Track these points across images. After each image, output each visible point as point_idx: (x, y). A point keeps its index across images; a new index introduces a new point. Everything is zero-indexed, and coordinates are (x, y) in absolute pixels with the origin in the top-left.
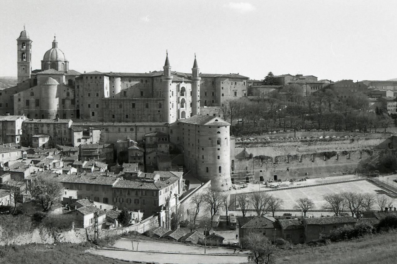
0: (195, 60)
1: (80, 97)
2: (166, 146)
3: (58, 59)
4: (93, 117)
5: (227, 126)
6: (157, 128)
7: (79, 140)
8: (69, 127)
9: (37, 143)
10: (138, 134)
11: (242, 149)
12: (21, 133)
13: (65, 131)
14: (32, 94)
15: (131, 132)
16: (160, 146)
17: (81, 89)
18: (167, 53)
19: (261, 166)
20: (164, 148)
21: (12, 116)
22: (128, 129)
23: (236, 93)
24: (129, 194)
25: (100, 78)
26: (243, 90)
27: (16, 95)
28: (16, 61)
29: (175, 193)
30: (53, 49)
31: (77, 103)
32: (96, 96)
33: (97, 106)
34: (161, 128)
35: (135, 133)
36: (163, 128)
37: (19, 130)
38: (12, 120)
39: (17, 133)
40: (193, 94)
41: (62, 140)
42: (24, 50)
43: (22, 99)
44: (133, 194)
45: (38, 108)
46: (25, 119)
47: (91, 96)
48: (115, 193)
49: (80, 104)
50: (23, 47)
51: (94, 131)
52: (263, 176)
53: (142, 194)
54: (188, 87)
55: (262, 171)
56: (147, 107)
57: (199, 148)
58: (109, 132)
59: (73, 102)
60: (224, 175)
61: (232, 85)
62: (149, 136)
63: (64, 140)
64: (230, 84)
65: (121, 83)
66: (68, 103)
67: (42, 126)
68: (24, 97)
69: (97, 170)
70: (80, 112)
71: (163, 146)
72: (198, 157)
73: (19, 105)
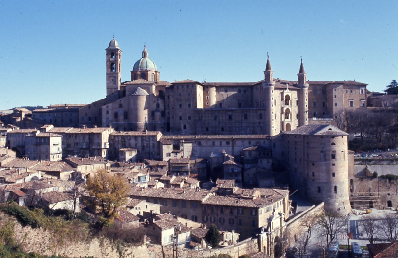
0: (301, 64)
2: (268, 162)
3: (148, 69)
5: (344, 137)
6: (257, 141)
7: (169, 155)
8: (158, 140)
9: (124, 157)
10: (235, 148)
11: (363, 167)
12: (108, 147)
13: (153, 144)
14: (121, 106)
15: (227, 145)
16: (261, 162)
17: (171, 99)
18: (268, 56)
19: (389, 188)
20: (266, 163)
21: (99, 129)
22: (224, 143)
23: (352, 103)
24: (222, 212)
26: (360, 99)
27: (104, 107)
29: (279, 212)
30: (143, 59)
31: (167, 115)
32: (187, 106)
33: (189, 118)
34: (262, 141)
35: (231, 147)
36: (264, 142)
37: (105, 143)
38: (98, 132)
39: (103, 146)
40: (300, 103)
41: (150, 154)
42: (113, 60)
43: (110, 112)
44: (227, 212)
46: (112, 131)
47: (182, 107)
48: (205, 210)
49: (171, 116)
51: (185, 145)
52: (392, 201)
53: (238, 212)
54: (293, 95)
55: (390, 194)
56: (246, 118)
57: (308, 164)
58: (201, 146)
59: (163, 114)
60: (341, 196)
61: (346, 94)
62: (247, 150)
63: (152, 154)
64: (345, 92)
65: (217, 94)
66: (158, 115)
67: (130, 139)
68: (112, 110)
69: (186, 186)
70: (171, 124)
71: (265, 161)
72: (308, 174)
73: (107, 119)
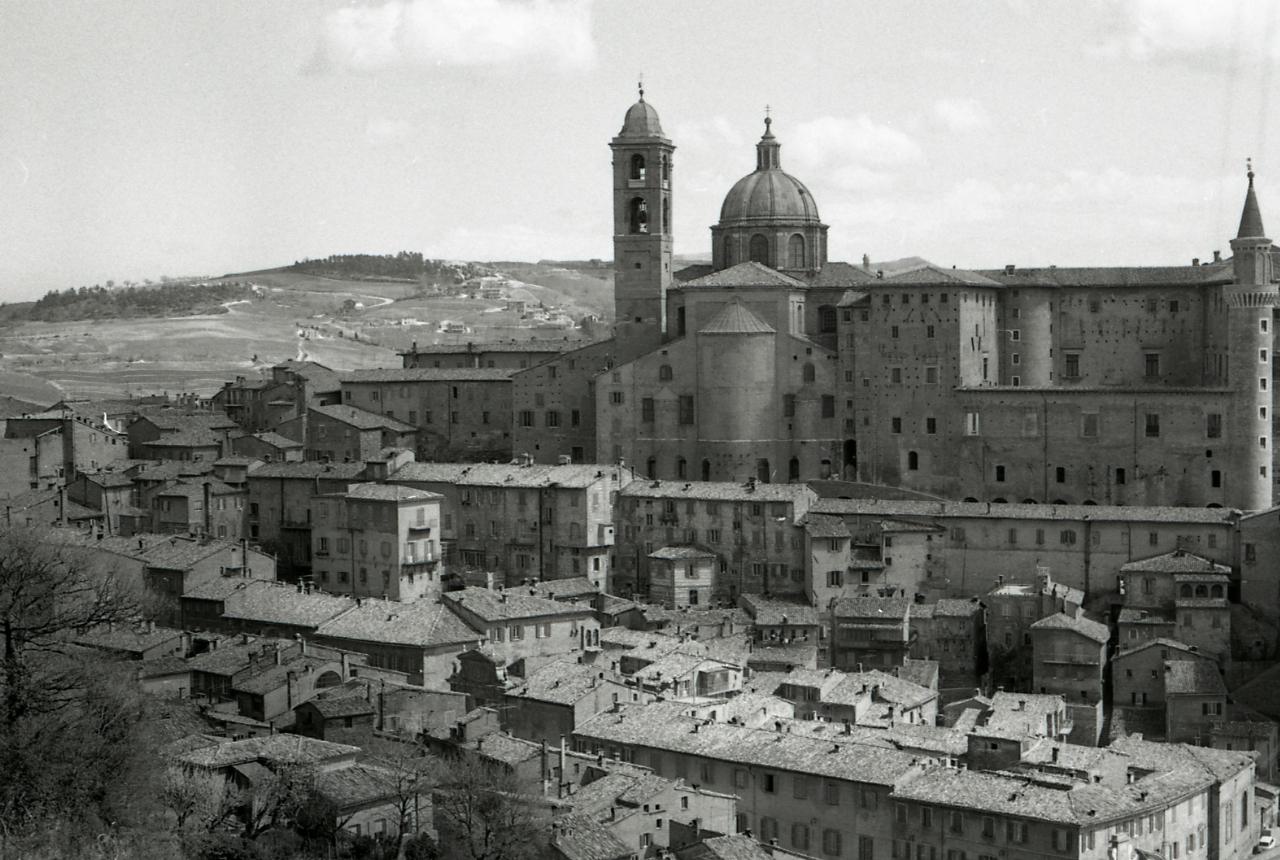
1: (859, 384)
2: (1216, 624)
4: (913, 472)
6: (1184, 533)
7: (835, 579)
8: (798, 517)
9: (667, 582)
10: (1094, 558)
12: (609, 540)
13: (779, 536)
14: (666, 374)
15: (1064, 547)
21: (577, 468)
22: (1052, 537)
24: (957, 829)
25: (944, 298)
27: (606, 379)
28: (611, 233)
30: (759, 174)
32: (923, 381)
33: (932, 425)
34: (1204, 534)
35: (1082, 555)
36: (1212, 537)
37: (601, 528)
38: (574, 484)
39: (592, 540)
41: (766, 571)
42: (643, 185)
43: (628, 396)
44: (975, 830)
45: (690, 432)
48: (902, 819)
49: (860, 418)
50: (637, 176)
53: (1010, 836)
56: (1153, 429)
58: (966, 547)
59: (828, 404)
62: (1138, 573)
63: (774, 575)
66: (809, 410)
67: (690, 512)
73: (617, 422)
